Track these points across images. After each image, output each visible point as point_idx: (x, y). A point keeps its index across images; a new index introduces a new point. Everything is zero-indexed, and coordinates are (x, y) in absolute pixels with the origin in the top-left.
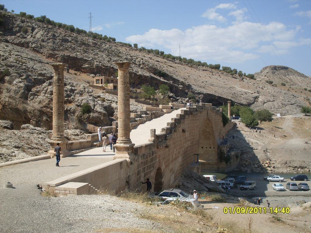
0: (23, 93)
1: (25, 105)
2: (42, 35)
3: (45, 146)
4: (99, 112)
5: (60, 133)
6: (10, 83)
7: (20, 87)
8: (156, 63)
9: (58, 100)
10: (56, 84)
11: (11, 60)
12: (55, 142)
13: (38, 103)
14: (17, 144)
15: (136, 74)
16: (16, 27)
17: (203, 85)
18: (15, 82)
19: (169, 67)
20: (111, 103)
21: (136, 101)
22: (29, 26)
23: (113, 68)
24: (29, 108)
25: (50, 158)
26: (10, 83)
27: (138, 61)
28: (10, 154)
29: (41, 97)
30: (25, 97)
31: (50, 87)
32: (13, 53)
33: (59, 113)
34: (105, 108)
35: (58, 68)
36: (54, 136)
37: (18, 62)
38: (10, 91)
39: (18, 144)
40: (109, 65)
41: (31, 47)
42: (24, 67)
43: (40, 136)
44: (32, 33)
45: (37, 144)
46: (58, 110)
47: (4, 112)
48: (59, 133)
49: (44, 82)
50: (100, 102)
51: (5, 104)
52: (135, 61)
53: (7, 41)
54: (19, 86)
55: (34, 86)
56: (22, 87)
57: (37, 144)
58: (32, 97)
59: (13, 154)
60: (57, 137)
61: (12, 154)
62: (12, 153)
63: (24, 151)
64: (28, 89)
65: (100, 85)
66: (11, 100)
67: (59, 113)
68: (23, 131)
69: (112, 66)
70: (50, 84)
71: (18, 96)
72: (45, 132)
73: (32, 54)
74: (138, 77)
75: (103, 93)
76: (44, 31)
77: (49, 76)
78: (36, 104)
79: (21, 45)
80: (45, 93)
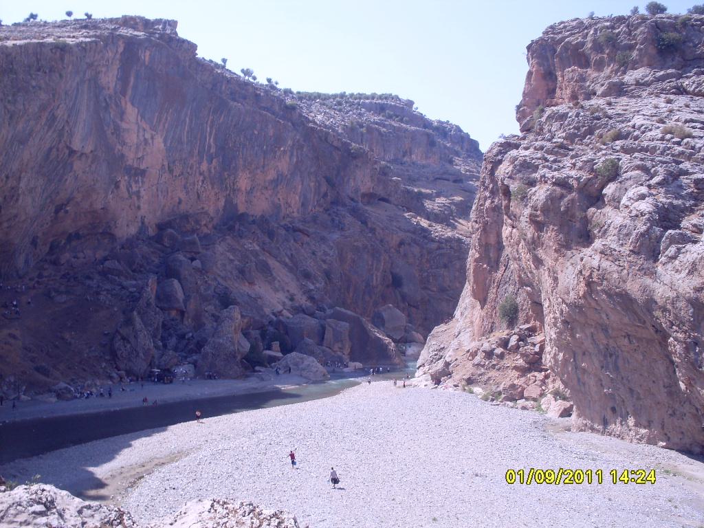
0: (642, 235)
1: (648, 281)
7: (637, 216)
13: (687, 271)
24: (661, 292)
26: (616, 202)
30: (649, 249)
32: (677, 117)
37: (668, 136)
38: (606, 230)
47: (593, 304)
51: (590, 276)
54: (634, 213)
56: (642, 214)
58: (672, 250)
66: (606, 264)
71: (626, 250)
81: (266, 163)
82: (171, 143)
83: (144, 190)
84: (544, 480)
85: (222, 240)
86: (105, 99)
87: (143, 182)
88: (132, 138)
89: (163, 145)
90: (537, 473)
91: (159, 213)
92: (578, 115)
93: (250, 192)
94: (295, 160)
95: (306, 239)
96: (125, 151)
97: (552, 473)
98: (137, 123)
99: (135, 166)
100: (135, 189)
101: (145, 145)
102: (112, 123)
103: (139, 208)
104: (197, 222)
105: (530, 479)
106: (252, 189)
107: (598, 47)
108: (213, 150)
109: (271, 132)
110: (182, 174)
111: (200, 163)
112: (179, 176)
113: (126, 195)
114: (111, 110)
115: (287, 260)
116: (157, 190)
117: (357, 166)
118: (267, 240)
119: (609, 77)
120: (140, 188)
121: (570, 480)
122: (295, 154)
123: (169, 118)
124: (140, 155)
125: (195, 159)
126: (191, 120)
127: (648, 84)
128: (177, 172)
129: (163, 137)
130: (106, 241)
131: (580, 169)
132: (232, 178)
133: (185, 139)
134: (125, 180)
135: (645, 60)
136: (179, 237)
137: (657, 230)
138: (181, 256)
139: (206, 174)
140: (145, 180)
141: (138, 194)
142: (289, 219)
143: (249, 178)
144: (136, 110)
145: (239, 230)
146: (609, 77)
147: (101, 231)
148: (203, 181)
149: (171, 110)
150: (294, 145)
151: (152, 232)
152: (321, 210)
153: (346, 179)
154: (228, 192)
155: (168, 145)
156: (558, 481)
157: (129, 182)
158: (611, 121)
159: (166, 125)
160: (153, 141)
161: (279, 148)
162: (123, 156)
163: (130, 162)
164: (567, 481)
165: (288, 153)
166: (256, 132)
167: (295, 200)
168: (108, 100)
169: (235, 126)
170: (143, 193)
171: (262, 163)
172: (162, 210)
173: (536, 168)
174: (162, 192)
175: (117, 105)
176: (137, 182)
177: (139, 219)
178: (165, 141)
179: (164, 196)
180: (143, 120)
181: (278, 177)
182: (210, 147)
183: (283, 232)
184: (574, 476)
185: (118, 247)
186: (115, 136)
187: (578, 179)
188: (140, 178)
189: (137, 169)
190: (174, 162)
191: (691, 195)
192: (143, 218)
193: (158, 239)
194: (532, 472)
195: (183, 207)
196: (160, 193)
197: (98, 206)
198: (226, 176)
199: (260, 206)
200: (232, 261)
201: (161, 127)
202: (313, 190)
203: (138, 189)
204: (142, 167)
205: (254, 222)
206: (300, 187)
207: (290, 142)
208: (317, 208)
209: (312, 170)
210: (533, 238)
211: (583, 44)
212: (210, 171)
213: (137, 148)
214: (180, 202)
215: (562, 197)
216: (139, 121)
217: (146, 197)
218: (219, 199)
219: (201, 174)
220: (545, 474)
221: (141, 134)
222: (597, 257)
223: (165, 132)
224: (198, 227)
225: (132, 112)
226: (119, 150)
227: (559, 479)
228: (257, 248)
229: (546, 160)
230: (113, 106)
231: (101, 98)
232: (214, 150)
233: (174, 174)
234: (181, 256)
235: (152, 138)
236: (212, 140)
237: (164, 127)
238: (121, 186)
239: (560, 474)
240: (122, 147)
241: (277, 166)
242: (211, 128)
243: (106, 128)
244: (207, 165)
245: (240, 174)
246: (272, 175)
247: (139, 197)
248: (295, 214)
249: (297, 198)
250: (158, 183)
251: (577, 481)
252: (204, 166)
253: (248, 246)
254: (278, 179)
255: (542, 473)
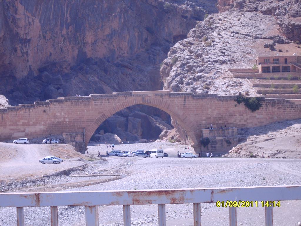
81: (104, 24)
82: (44, 21)
83: (30, 51)
84: (233, 205)
85: (76, 76)
86: (7, 5)
87: (29, 46)
88: (22, 23)
89: (39, 24)
90: (230, 203)
91: (39, 63)
93: (94, 44)
94: (123, 20)
95: (131, 72)
96: (19, 31)
97: (236, 202)
98: (24, 14)
99: (25, 38)
100: (25, 51)
101: (30, 25)
102: (11, 16)
103: (28, 61)
104: (61, 67)
105: (226, 205)
106: (95, 41)
108: (69, 21)
109: (105, 5)
110: (51, 38)
111: (61, 30)
112: (50, 39)
113: (21, 55)
114: (10, 10)
115: (115, 86)
116: (37, 50)
117: (169, 18)
118: (103, 74)
120: (28, 49)
121: (243, 206)
122: (122, 16)
123: (42, 8)
124: (27, 31)
125: (58, 28)
126: (55, 6)
128: (48, 37)
129: (39, 19)
130: (11, 80)
132: (82, 36)
133: (52, 17)
134: (20, 47)
136: (51, 76)
138: (52, 88)
139: (66, 36)
140: (30, 45)
141: (27, 53)
142: (120, 59)
143: (93, 35)
144: (23, 7)
145: (86, 69)
147: (8, 75)
148: (64, 41)
149: (42, 4)
150: (121, 11)
151: (35, 74)
152: (144, 50)
153: (162, 27)
154: (80, 45)
155: (42, 23)
156: (239, 206)
157: (22, 48)
159: (40, 12)
160: (33, 23)
161: (111, 15)
162: (17, 34)
163: (22, 36)
164: (242, 206)
165: (118, 17)
166: (96, 6)
167: (125, 45)
168: (8, 5)
169: (82, 4)
170: (29, 52)
171: (101, 25)
172: (41, 60)
174: (40, 50)
175: (13, 6)
176: (26, 46)
177: (28, 67)
178: (40, 22)
179: (41, 53)
180: (27, 12)
181: (112, 32)
182: (67, 19)
183: (114, 68)
184: (245, 204)
185: (18, 84)
186: (13, 23)
188: (27, 44)
189: (26, 39)
190: (46, 32)
192: (30, 66)
193: (39, 78)
194: (227, 202)
195: (53, 57)
196: (39, 51)
197: (7, 62)
198: (78, 36)
199: (102, 51)
200: (81, 88)
201: (38, 13)
202: (137, 38)
203: (26, 50)
204: (29, 38)
205: (96, 63)
206: (128, 37)
207: (119, 10)
208: (141, 49)
209: (136, 25)
212: (68, 34)
213: (25, 28)
214: (51, 54)
216: (25, 13)
217: (31, 55)
218: (74, 50)
219: (62, 36)
220: (233, 203)
221: (27, 20)
223: (40, 17)
224: (62, 69)
225: (21, 8)
226: (15, 31)
227: (239, 205)
228: (97, 79)
230: (11, 7)
231: (5, 4)
232: (70, 20)
233: (46, 39)
234: (52, 88)
235: (33, 21)
236: (68, 15)
237: (39, 13)
238: (18, 50)
239: (239, 203)
240: (17, 29)
241: (111, 26)
242: (67, 8)
243: (8, 20)
244: (66, 30)
245: (87, 33)
246: (108, 31)
247: (27, 55)
248: (126, 55)
249: (126, 44)
250: (37, 46)
251: (247, 206)
252: (64, 31)
253: (91, 79)
254: (112, 34)
255: (232, 203)
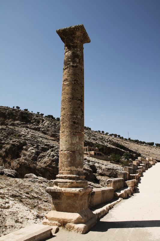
0: (34, 156)
2: (48, 124)
3: (45, 195)
4: (86, 170)
5: (77, 167)
6: (26, 150)
8: (117, 141)
9: (72, 94)
10: (68, 64)
11: (29, 136)
12: (63, 189)
14: (14, 193)
15: (106, 146)
16: (33, 120)
17: (147, 154)
18: (29, 150)
19: (124, 143)
20: (94, 163)
21: (111, 162)
22: (40, 119)
23: (92, 143)
25: (51, 236)
26: (26, 150)
27: (107, 139)
28: (3, 205)
29: (46, 159)
31: (52, 152)
33: (74, 123)
34: (91, 167)
35: (73, 35)
36: (62, 175)
37: (32, 138)
39: (16, 192)
40: (90, 141)
41: (41, 131)
42: (36, 140)
43: (42, 185)
44: (42, 123)
45: (37, 193)
46: (71, 115)
47: (21, 169)
48: (74, 168)
49: (48, 150)
50: (87, 163)
51: (22, 164)
52: (105, 139)
53: (27, 127)
55: (41, 153)
56: (33, 153)
57: (37, 193)
58: (40, 159)
59: (7, 205)
60: (70, 178)
61: (4, 205)
62: (5, 204)
63: (21, 201)
64: (37, 153)
65: (86, 152)
66: (26, 161)
67: (74, 123)
68: (25, 179)
69: (91, 142)
70: (52, 151)
71: (30, 159)
72: (46, 181)
73: (41, 134)
74: (108, 148)
75: (88, 157)
76: (49, 121)
77: (52, 146)
78: (42, 164)
79: (35, 129)
80: (49, 157)
92: (8, 130)
107: (9, 114)
119: (11, 121)
127: (20, 125)
131: (17, 142)
135: (19, 119)
137: (36, 156)
146: (11, 121)
158: (17, 132)
173: (2, 140)
187: (17, 145)
191: (41, 150)
210: (4, 156)
211: (5, 113)
215: (13, 148)
222: (24, 160)
229: (4, 139)
